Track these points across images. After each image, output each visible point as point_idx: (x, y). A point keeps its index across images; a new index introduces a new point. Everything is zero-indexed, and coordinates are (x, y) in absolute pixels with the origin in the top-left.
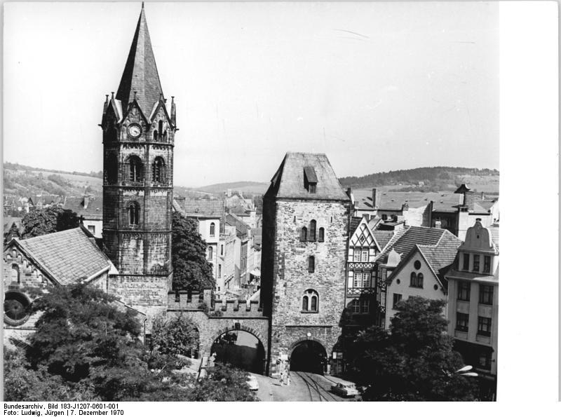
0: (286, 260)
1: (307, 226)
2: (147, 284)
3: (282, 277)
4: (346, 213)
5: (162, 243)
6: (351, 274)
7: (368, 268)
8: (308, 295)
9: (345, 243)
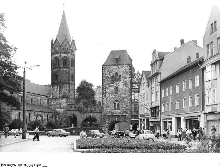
0: (106, 89)
1: (114, 75)
4: (130, 69)
5: (67, 87)
7: (136, 91)
9: (130, 81)
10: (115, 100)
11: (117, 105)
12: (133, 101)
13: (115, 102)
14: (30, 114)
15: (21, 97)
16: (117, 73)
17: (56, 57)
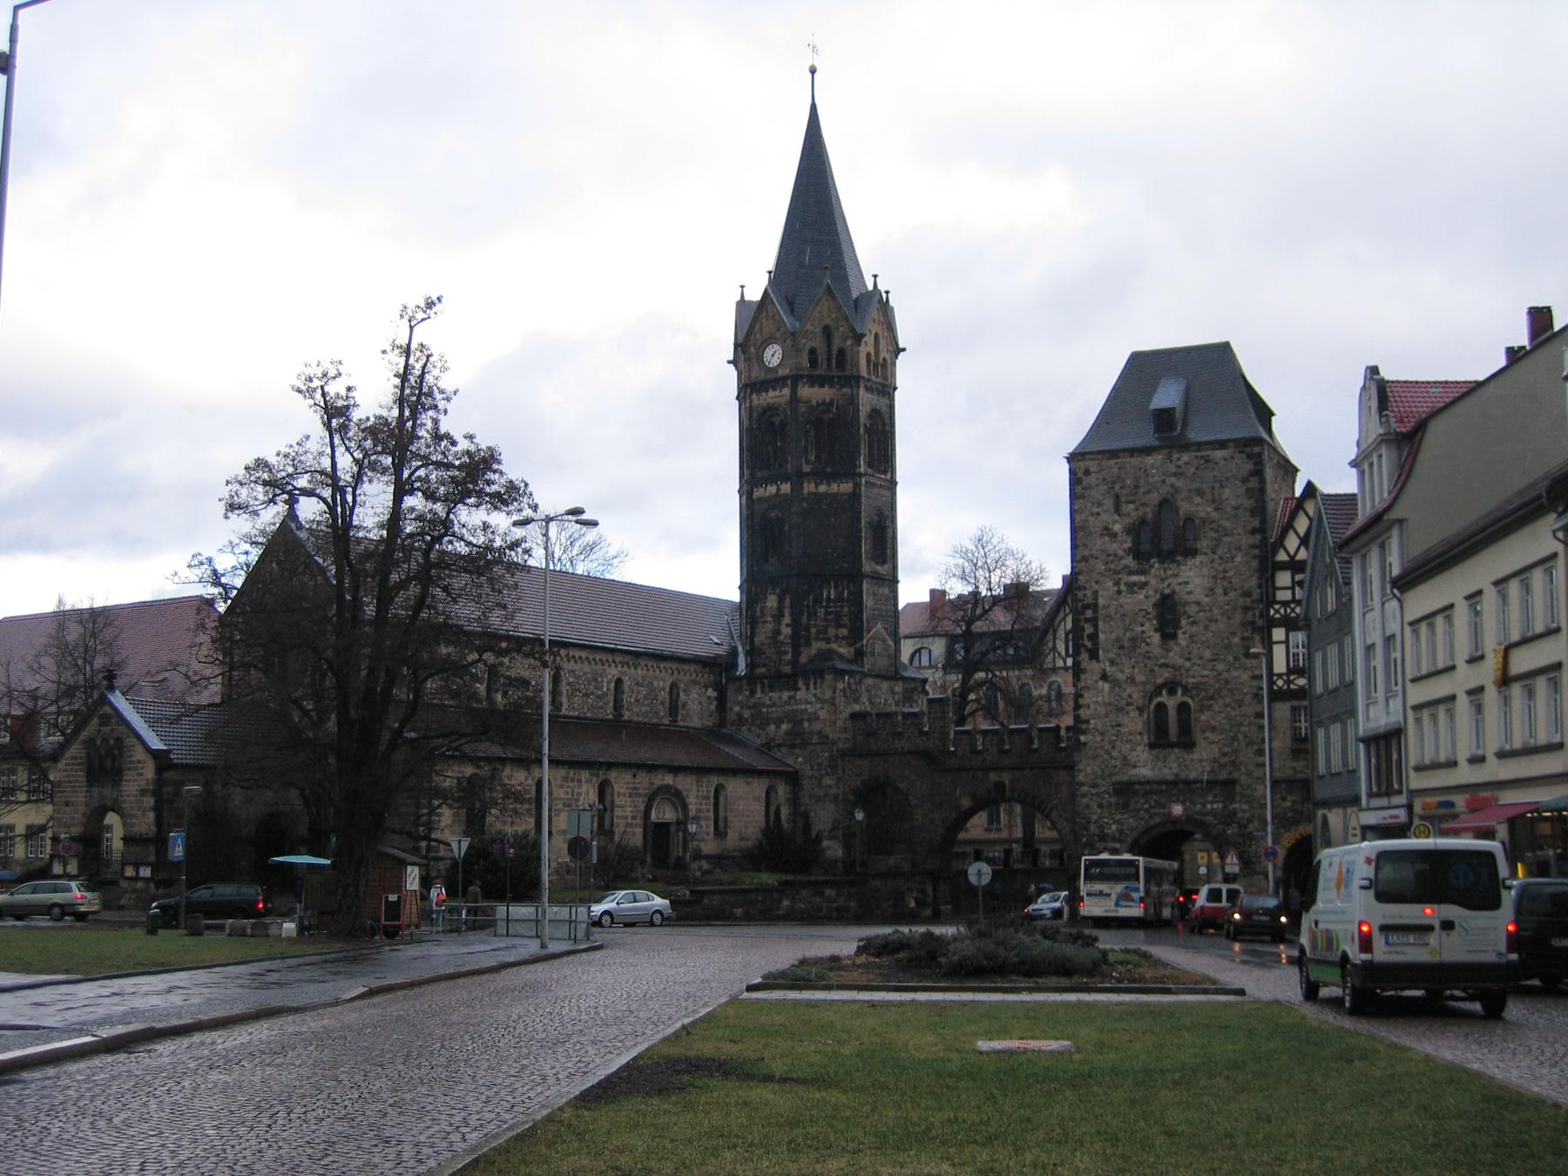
2: (801, 694)
3: (1094, 655)
6: (1278, 634)
8: (1164, 698)
10: (1160, 681)
11: (1172, 712)
12: (1280, 683)
13: (1157, 691)
14: (603, 788)
16: (1166, 504)
17: (771, 409)
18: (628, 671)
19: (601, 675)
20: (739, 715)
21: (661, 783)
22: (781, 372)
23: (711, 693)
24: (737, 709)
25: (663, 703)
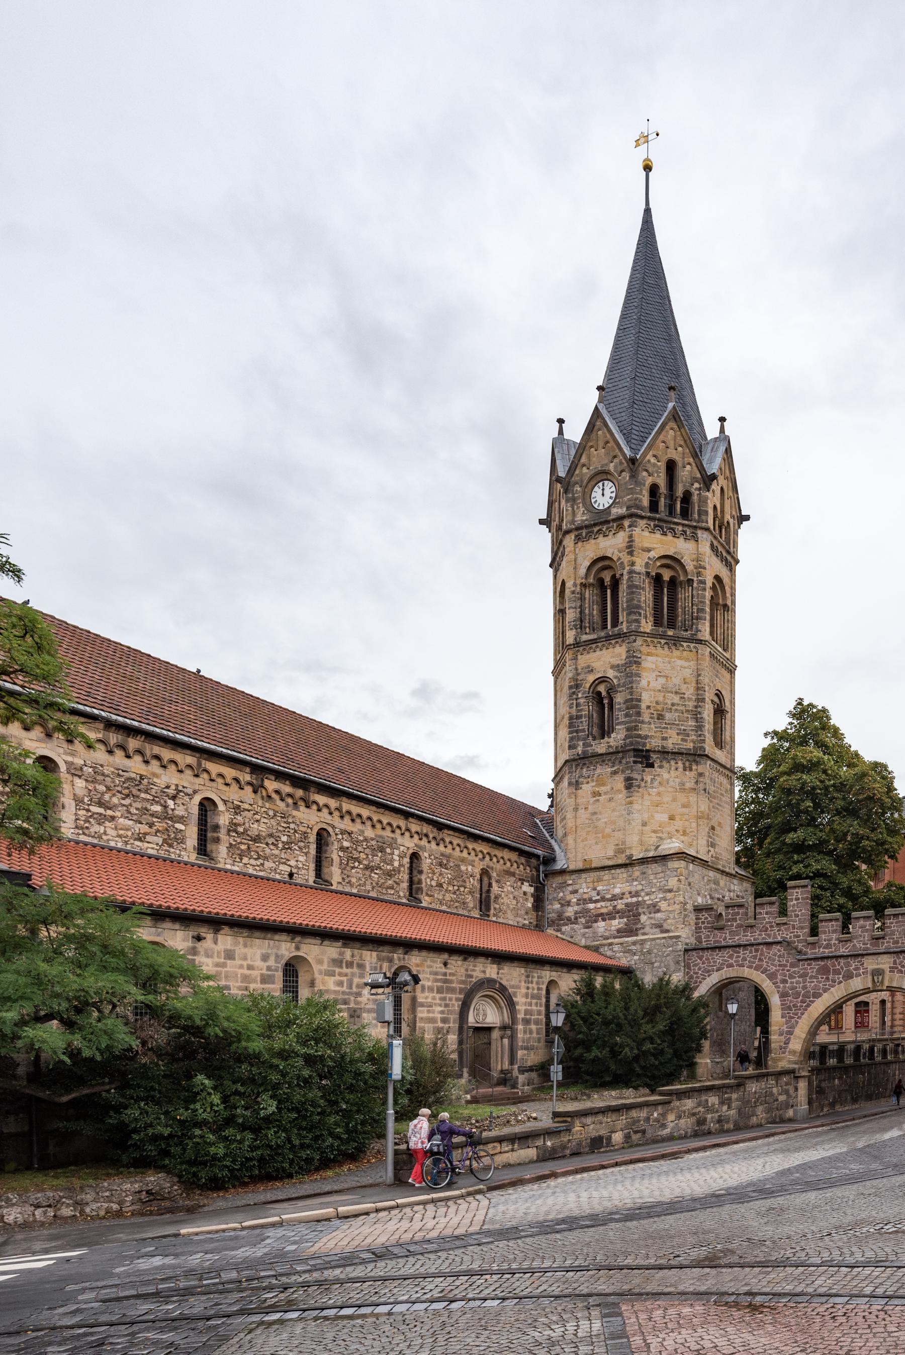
15: (313, 838)
18: (427, 845)
19: (390, 846)
20: (560, 916)
21: (481, 976)
22: (617, 511)
23: (527, 888)
24: (557, 906)
25: (471, 893)
